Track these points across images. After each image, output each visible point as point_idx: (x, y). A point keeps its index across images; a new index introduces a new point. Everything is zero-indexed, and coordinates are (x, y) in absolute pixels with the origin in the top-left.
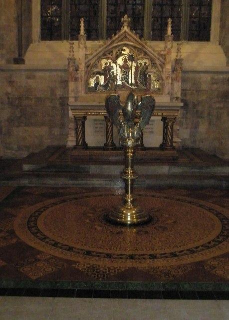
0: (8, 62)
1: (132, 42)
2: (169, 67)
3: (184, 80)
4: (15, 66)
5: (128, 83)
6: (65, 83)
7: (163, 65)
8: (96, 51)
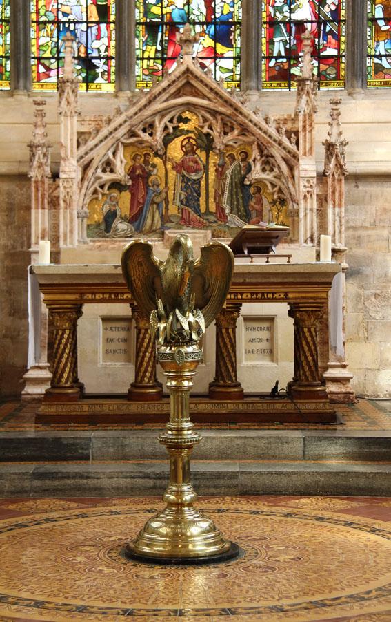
1: (204, 97)
5: (197, 210)
7: (292, 162)
8: (109, 121)
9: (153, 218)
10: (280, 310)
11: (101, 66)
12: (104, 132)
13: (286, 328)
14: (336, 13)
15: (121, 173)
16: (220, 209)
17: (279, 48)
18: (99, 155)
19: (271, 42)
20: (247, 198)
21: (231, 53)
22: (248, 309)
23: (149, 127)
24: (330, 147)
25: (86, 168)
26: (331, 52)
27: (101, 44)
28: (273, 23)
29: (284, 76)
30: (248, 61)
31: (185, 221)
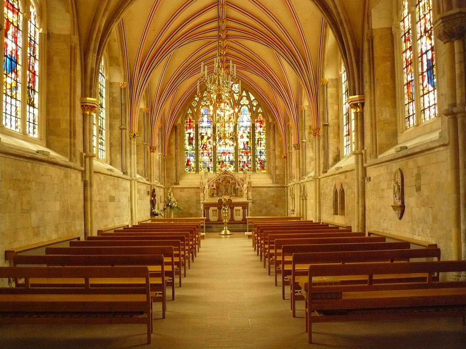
2: (245, 186)
3: (253, 191)
4: (175, 186)
6: (198, 194)
9: (220, 194)
10: (240, 208)
11: (211, 169)
12: (212, 180)
13: (242, 211)
15: (215, 187)
17: (241, 165)
18: (211, 185)
19: (240, 164)
20: (236, 191)
22: (235, 208)
23: (219, 179)
24: (249, 182)
25: (209, 186)
26: (250, 166)
27: (211, 165)
28: (240, 161)
29: (242, 170)
31: (225, 195)
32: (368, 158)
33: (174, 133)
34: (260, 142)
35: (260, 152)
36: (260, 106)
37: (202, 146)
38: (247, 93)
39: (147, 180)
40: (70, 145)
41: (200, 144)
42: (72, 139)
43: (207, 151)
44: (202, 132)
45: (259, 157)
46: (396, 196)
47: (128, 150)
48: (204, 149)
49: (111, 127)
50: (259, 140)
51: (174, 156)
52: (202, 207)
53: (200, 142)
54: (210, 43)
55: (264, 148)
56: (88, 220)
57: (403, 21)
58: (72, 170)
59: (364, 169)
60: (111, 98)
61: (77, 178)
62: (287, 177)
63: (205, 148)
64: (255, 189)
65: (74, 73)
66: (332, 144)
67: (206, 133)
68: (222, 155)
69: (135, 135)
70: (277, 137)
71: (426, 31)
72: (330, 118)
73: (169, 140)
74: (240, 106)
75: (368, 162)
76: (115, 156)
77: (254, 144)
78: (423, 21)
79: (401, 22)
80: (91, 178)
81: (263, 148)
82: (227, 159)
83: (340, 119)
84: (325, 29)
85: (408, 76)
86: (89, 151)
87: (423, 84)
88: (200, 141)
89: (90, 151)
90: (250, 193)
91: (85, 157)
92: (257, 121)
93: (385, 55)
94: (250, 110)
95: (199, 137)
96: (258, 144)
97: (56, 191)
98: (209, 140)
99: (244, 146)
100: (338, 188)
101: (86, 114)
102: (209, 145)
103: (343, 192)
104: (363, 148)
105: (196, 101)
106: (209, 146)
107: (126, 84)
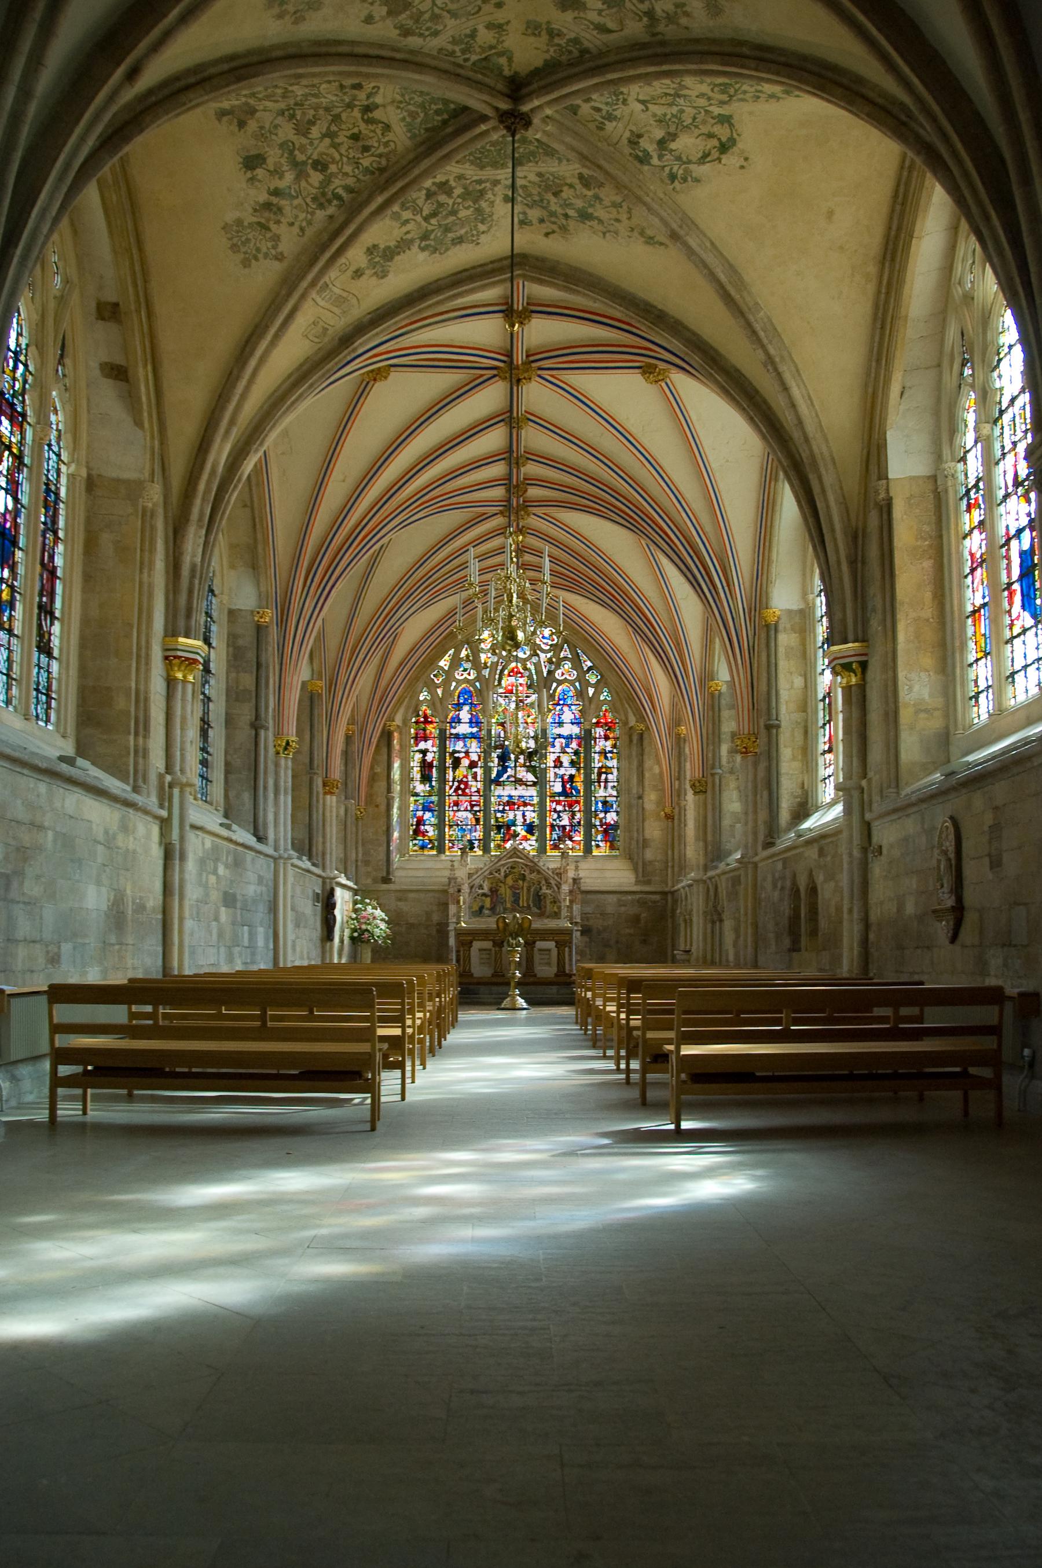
0: (375, 881)
2: (565, 888)
3: (584, 902)
4: (385, 887)
6: (444, 906)
9: (499, 908)
10: (551, 945)
11: (476, 843)
14: (579, 823)
15: (486, 890)
16: (529, 905)
17: (555, 836)
18: (477, 882)
21: (534, 838)
22: (540, 944)
23: (498, 871)
24: (574, 880)
25: (471, 887)
30: (542, 840)
32: (876, 798)
33: (385, 750)
34: (603, 776)
35: (605, 803)
36: (607, 685)
37: (456, 784)
38: (573, 649)
39: (314, 865)
40: (136, 752)
41: (451, 779)
42: (141, 740)
43: (468, 798)
44: (457, 749)
45: (602, 815)
46: (942, 886)
47: (271, 782)
48: (460, 792)
49: (229, 721)
50: (604, 770)
51: (383, 808)
52: (452, 941)
53: (450, 775)
54: (482, 518)
55: (615, 793)
56: (172, 944)
57: (963, 459)
58: (139, 814)
59: (867, 828)
60: (231, 649)
61: (148, 837)
62: (673, 867)
63: (463, 790)
64: (589, 896)
65: (149, 576)
66: (787, 774)
67: (467, 753)
68: (507, 808)
69: (288, 743)
70: (648, 763)
71: (1017, 484)
72: (783, 709)
73: (372, 768)
74: (555, 685)
75: (875, 806)
76: (238, 796)
77: (588, 783)
78: (1010, 458)
79: (959, 461)
80: (182, 838)
81: (610, 791)
82: (520, 820)
83: (809, 710)
84: (773, 483)
85: (976, 593)
86: (181, 770)
87: (1009, 612)
88: (451, 773)
89: (182, 771)
90: (576, 908)
91: (171, 786)
92: (598, 725)
93: (919, 543)
94: (581, 694)
95: (449, 762)
96: (599, 782)
97: (99, 860)
98: (474, 770)
99: (564, 786)
100: (802, 882)
101: (176, 679)
102: (474, 783)
103: (813, 890)
104: (864, 775)
105: (442, 668)
106: (475, 786)
107: (269, 616)
